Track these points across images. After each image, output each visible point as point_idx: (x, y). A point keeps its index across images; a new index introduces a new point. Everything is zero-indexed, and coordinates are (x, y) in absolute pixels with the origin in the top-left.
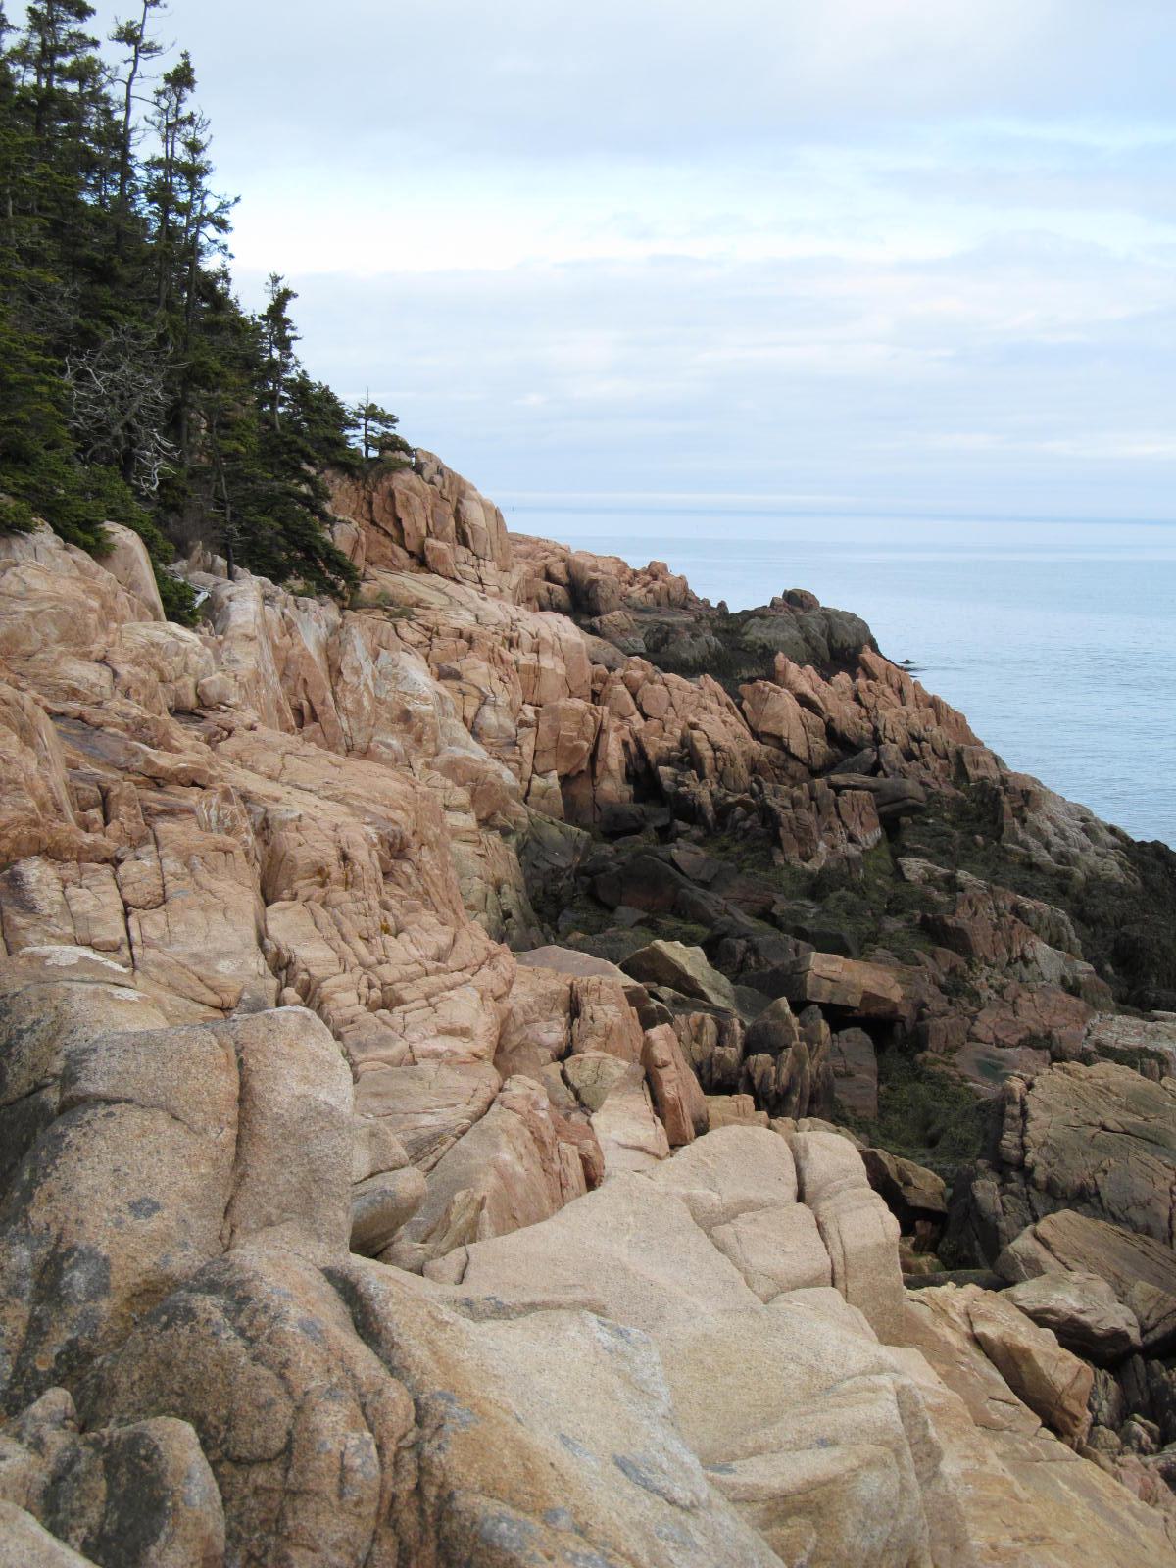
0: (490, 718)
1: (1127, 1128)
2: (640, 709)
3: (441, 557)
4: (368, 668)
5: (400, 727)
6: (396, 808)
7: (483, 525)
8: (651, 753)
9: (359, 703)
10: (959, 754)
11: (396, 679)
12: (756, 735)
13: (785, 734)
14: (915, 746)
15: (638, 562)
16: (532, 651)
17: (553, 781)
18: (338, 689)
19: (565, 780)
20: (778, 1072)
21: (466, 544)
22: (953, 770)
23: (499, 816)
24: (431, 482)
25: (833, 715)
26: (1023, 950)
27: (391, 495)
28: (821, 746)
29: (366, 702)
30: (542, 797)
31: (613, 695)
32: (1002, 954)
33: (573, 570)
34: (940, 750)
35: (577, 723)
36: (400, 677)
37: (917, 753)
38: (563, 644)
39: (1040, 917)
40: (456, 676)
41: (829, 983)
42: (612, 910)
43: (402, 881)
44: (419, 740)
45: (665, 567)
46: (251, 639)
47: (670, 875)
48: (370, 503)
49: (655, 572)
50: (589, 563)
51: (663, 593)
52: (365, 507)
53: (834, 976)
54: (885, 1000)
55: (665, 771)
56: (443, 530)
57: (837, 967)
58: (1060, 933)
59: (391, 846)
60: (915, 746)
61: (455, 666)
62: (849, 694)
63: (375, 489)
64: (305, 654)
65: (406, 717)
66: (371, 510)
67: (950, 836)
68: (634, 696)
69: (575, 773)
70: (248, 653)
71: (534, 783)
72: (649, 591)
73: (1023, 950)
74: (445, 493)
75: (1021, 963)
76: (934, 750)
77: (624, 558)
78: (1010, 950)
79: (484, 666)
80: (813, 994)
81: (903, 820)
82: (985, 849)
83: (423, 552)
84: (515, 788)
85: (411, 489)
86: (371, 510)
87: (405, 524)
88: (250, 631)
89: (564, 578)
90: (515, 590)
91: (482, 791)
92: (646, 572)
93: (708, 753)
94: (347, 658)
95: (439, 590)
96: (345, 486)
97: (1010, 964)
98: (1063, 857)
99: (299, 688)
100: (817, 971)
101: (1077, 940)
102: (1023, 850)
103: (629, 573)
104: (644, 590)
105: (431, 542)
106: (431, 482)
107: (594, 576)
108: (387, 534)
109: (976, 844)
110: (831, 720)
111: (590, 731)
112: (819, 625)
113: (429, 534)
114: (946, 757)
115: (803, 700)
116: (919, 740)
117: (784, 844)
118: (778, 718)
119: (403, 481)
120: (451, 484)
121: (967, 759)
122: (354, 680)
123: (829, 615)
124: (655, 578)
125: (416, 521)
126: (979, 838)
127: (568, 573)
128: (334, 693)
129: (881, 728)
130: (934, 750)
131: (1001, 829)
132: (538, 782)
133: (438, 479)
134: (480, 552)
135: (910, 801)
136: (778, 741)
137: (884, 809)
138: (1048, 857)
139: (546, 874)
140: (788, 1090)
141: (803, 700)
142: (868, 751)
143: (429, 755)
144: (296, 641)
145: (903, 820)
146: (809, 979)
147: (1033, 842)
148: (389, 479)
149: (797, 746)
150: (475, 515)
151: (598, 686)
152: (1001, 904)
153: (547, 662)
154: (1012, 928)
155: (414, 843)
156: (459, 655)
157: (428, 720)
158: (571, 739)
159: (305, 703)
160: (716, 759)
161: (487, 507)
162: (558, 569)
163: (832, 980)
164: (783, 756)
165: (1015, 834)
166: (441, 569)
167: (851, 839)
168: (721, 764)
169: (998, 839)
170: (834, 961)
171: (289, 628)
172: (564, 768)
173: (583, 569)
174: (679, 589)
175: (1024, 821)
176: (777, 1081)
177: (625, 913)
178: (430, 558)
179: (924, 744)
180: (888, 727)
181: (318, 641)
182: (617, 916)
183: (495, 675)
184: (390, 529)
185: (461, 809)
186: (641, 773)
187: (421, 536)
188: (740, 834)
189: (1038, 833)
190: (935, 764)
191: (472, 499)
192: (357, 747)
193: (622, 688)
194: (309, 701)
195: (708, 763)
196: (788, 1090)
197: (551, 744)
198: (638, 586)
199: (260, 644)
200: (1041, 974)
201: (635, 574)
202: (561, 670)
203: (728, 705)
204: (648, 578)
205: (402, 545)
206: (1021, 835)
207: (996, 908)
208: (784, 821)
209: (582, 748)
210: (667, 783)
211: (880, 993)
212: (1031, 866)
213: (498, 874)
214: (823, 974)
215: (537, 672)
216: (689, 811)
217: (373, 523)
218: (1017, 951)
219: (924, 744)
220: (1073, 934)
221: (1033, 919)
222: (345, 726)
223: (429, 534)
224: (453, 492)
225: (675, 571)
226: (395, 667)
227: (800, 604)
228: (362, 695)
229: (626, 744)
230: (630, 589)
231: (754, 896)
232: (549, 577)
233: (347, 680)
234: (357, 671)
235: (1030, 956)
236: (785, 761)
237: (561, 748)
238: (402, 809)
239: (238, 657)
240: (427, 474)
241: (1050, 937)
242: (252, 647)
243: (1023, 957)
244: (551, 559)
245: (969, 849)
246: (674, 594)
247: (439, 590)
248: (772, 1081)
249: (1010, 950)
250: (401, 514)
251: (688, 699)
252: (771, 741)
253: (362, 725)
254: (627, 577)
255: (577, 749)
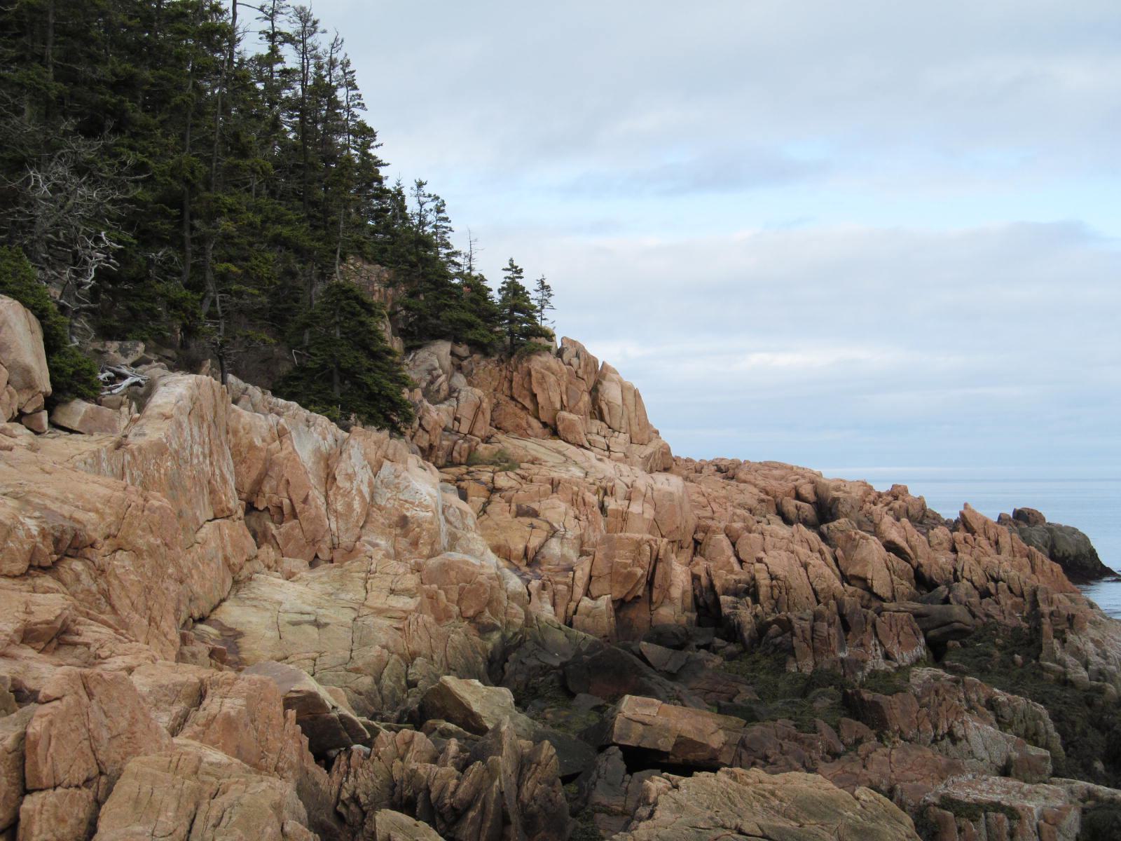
0: (555, 547)
1: (767, 832)
2: (737, 555)
3: (571, 426)
4: (364, 475)
5: (398, 531)
6: (90, 511)
7: (620, 402)
8: (718, 584)
9: (349, 506)
10: (1034, 593)
11: (398, 488)
12: (845, 578)
13: (870, 577)
14: (991, 585)
15: (883, 488)
16: (625, 499)
17: (604, 603)
18: (331, 493)
19: (620, 605)
20: (457, 786)
21: (602, 419)
22: (1028, 607)
23: (487, 614)
24: (570, 364)
25: (921, 561)
26: (950, 728)
27: (529, 374)
28: (906, 587)
29: (357, 505)
30: (588, 616)
31: (712, 543)
32: (926, 730)
33: (819, 491)
34: (1017, 590)
35: (631, 551)
36: (402, 487)
37: (993, 591)
38: (655, 493)
39: (1014, 710)
40: (535, 514)
41: (641, 727)
42: (572, 695)
43: (68, 577)
44: (415, 544)
45: (906, 490)
46: (166, 417)
47: (635, 665)
48: (511, 381)
49: (897, 493)
50: (833, 485)
51: (902, 510)
52: (506, 385)
53: (647, 720)
54: (703, 746)
55: (724, 599)
56: (577, 404)
57: (653, 711)
58: (1037, 725)
59: (57, 541)
60: (991, 585)
61: (535, 506)
62: (946, 545)
63: (516, 369)
64: (293, 457)
65: (404, 522)
66: (511, 388)
67: (989, 655)
68: (734, 544)
69: (630, 598)
70: (159, 429)
71: (582, 604)
72: (891, 510)
73: (950, 728)
74: (580, 373)
75: (946, 742)
76: (1009, 588)
77: (869, 483)
78: (936, 727)
79: (563, 506)
80: (620, 737)
81: (950, 643)
82: (1022, 666)
83: (555, 424)
84: (520, 594)
85: (548, 369)
86: (511, 388)
87: (540, 399)
88: (167, 410)
89: (811, 497)
90: (647, 458)
91: (470, 591)
92: (888, 494)
93: (763, 580)
94: (342, 465)
95: (559, 452)
96: (490, 367)
97: (935, 741)
98: (1101, 675)
99: (281, 487)
100: (628, 713)
101: (1056, 734)
102: (1061, 668)
103: (874, 494)
104: (886, 508)
105: (565, 414)
106: (570, 364)
107: (836, 494)
108: (524, 408)
109: (1014, 662)
110: (920, 565)
111: (646, 560)
112: (1042, 537)
113: (563, 407)
114: (1022, 596)
115: (891, 547)
116: (996, 581)
117: (797, 653)
118: (864, 562)
119: (538, 363)
120: (586, 365)
121: (1040, 597)
122: (348, 485)
123: (1051, 529)
124: (896, 498)
125: (551, 395)
126: (1018, 658)
127: (816, 493)
128: (327, 497)
129: (959, 569)
130: (1009, 588)
131: (1040, 648)
132: (586, 602)
133: (575, 361)
134: (616, 425)
135: (957, 625)
136: (863, 582)
137: (932, 633)
138: (1085, 674)
139: (533, 668)
140: (469, 806)
141: (891, 547)
142: (941, 588)
143: (421, 556)
144: (284, 447)
145: (950, 643)
146: (617, 722)
147: (1069, 660)
148: (529, 361)
149: (880, 587)
150: (612, 393)
151: (700, 536)
152: (973, 696)
153: (636, 508)
154: (940, 705)
155: (104, 547)
156: (541, 496)
157: (426, 525)
158: (625, 566)
159: (286, 502)
160: (772, 587)
161: (625, 388)
162: (807, 490)
163: (644, 724)
164: (867, 596)
165: (1053, 652)
166: (570, 438)
167: (887, 656)
168: (776, 591)
169: (1037, 658)
170: (648, 705)
171: (281, 434)
172: (618, 593)
173: (827, 490)
174: (917, 507)
175: (1064, 641)
176: (454, 793)
177: (581, 697)
178: (560, 428)
179: (1001, 583)
180: (966, 568)
181: (317, 451)
182: (575, 703)
183: (572, 513)
184: (528, 403)
185: (407, 592)
186: (706, 604)
187: (556, 411)
188: (772, 649)
189: (1077, 653)
190: (1007, 601)
191: (612, 380)
192: (343, 545)
193: (722, 537)
194: (291, 500)
195: (763, 591)
196: (469, 806)
197: (606, 571)
198: (880, 505)
199: (180, 425)
200: (971, 753)
201: (880, 495)
202: (649, 514)
203: (821, 552)
204: (890, 498)
205: (537, 418)
206: (1058, 654)
207: (968, 700)
208: (798, 631)
209: (635, 575)
210: (726, 610)
211: (697, 739)
212: (1065, 683)
213: (414, 646)
214: (634, 717)
215: (624, 517)
216: (731, 631)
217: (512, 398)
218: (943, 727)
219: (1001, 583)
220: (1051, 727)
221: (1007, 711)
222: (333, 526)
223: (563, 407)
224: (594, 378)
225: (914, 492)
226: (397, 477)
227: (1027, 521)
228: (353, 499)
229: (695, 578)
230: (874, 507)
231: (720, 688)
232: (798, 496)
233: (341, 485)
234: (350, 477)
235: (959, 732)
236: (869, 600)
237: (617, 575)
238: (97, 511)
239: (147, 432)
240: (565, 357)
241: (1027, 730)
242: (166, 425)
243: (950, 734)
244: (802, 481)
245: (1007, 667)
246: (911, 511)
247: (559, 452)
248: (448, 794)
249: (936, 727)
250: (536, 390)
251: (778, 545)
252: (858, 583)
253: (350, 526)
254: (871, 498)
255: (631, 575)
